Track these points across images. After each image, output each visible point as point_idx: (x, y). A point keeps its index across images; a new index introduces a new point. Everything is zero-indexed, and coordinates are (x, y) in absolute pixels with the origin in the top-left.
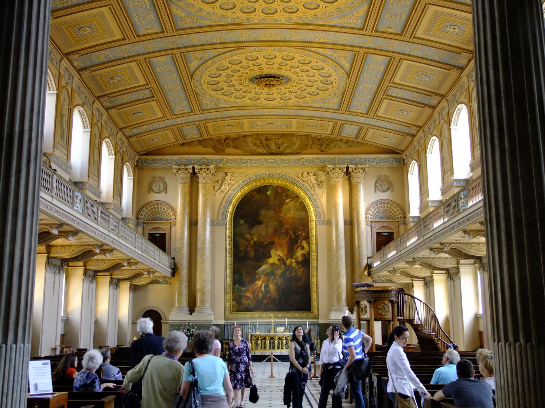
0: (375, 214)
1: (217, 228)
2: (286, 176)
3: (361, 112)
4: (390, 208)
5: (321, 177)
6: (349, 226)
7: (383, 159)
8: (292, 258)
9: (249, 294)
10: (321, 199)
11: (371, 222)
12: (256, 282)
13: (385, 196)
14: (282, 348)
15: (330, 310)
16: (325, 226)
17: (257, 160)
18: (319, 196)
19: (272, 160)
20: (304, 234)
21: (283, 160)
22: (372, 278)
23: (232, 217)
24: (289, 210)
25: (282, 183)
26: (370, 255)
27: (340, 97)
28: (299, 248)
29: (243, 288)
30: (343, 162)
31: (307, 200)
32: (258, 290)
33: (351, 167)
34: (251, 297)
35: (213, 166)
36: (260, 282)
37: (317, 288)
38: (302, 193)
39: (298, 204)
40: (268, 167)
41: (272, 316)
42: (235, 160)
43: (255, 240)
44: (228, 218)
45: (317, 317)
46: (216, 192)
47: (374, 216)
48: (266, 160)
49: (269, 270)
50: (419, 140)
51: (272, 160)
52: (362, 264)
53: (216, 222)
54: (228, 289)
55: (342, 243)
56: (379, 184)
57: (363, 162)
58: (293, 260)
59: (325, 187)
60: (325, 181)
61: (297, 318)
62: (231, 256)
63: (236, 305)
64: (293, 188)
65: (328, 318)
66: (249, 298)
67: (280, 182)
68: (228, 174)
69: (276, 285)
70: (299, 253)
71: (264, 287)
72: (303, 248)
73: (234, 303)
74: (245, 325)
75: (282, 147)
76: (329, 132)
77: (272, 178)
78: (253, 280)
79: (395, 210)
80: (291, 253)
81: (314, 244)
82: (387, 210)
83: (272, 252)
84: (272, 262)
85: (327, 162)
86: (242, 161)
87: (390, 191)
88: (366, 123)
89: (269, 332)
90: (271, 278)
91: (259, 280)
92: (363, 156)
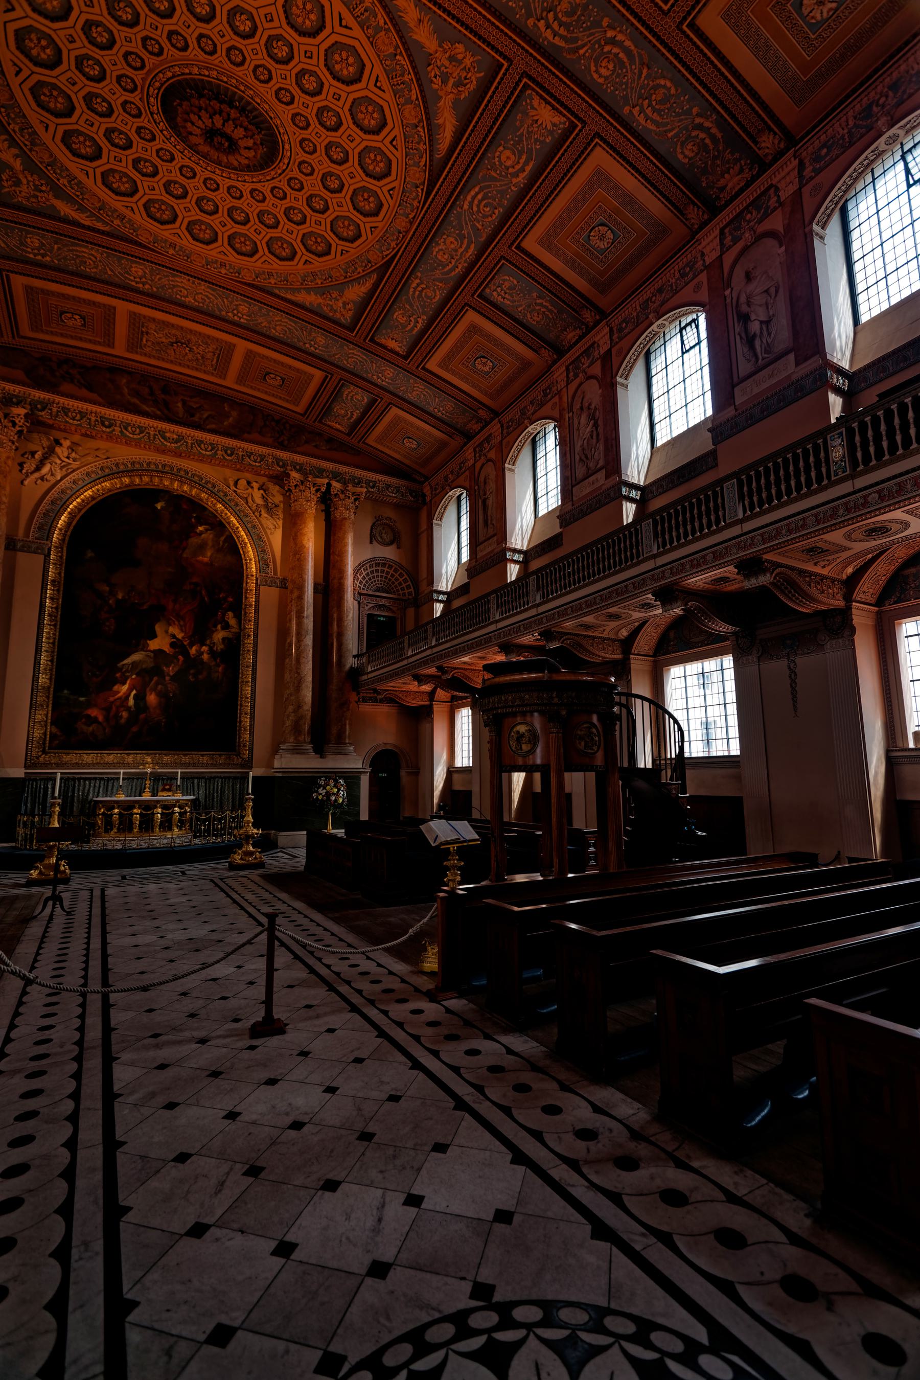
0: (367, 582)
1: (23, 559)
2: (201, 479)
3: (398, 349)
4: (392, 576)
5: (274, 496)
6: (320, 596)
7: (389, 486)
8: (203, 644)
9: (94, 712)
10: (270, 537)
11: (360, 594)
12: (116, 688)
13: (389, 553)
14: (170, 829)
15: (275, 750)
16: (277, 589)
17: (139, 427)
18: (269, 532)
19: (175, 437)
20: (230, 599)
21: (200, 442)
22: (358, 694)
23: (63, 540)
24: (202, 547)
25: (191, 491)
26: (355, 653)
27: (375, 276)
28: (219, 627)
29: (82, 699)
30: (320, 472)
31: (243, 533)
32: (118, 704)
33: (336, 485)
34: (101, 719)
35: (22, 411)
36: (125, 688)
37: (253, 707)
38: (232, 519)
39: (223, 538)
40: (163, 451)
41: (149, 760)
42: (83, 415)
43: (120, 596)
44: (54, 539)
45: (249, 764)
46: (27, 476)
47: (365, 586)
48: (162, 433)
49: (150, 664)
50: (480, 445)
51: (175, 437)
52: (344, 666)
53: (19, 545)
54: (41, 698)
55: (309, 623)
56: (378, 529)
57: (358, 482)
58: (204, 648)
59: (281, 516)
60: (282, 505)
61: (207, 766)
62: (55, 625)
63: (59, 733)
64: (214, 505)
65: (270, 765)
66: (93, 720)
67: (185, 488)
68: (62, 441)
69: (162, 695)
70: (219, 635)
71: (134, 698)
72: (226, 626)
73: (54, 730)
74: (79, 779)
75: (198, 415)
76: (300, 409)
77: (169, 476)
78: (109, 683)
79: (401, 580)
80: (200, 635)
81: (250, 621)
82: (386, 578)
83: (158, 628)
84: (157, 647)
85: (289, 468)
86: (102, 420)
87: (394, 546)
88: (391, 388)
89: (140, 795)
90: (151, 680)
91: (124, 684)
92: (358, 473)
